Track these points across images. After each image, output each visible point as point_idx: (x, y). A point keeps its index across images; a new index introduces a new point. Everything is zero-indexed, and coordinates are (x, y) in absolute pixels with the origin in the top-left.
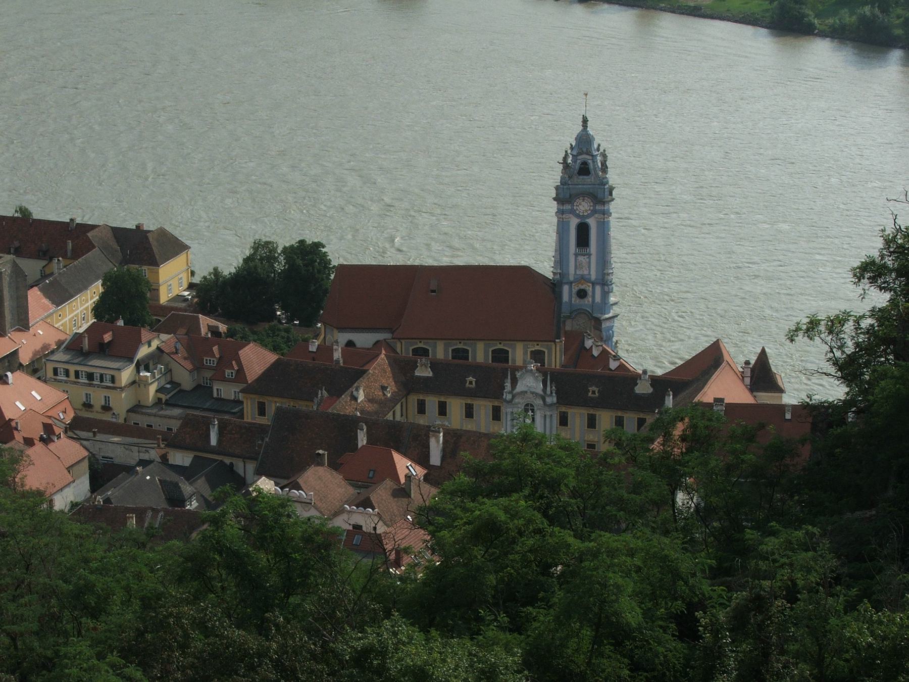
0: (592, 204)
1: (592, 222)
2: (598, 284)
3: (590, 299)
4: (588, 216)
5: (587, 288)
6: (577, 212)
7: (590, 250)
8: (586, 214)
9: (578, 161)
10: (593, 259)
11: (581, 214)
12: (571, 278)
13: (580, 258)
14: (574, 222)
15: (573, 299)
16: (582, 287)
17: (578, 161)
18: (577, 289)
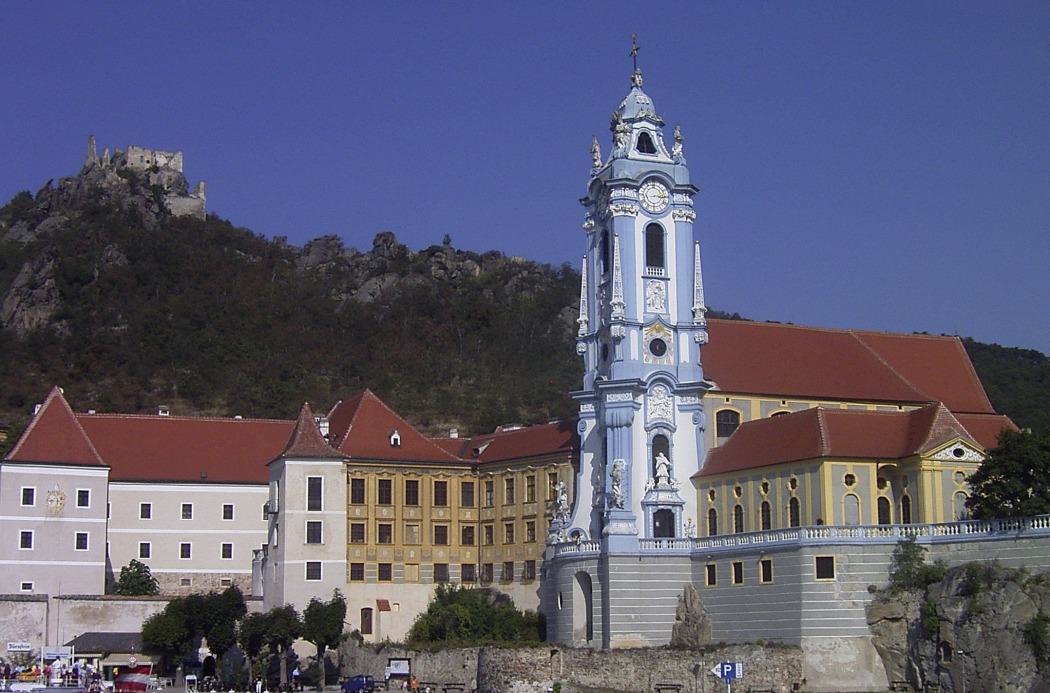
0: (667, 193)
1: (668, 224)
2: (684, 328)
3: (672, 359)
4: (662, 214)
5: (665, 339)
6: (645, 205)
7: (666, 273)
8: (657, 210)
9: (635, 132)
10: (672, 284)
11: (651, 209)
13: (653, 286)
14: (641, 222)
15: (645, 356)
17: (635, 132)
18: (651, 339)
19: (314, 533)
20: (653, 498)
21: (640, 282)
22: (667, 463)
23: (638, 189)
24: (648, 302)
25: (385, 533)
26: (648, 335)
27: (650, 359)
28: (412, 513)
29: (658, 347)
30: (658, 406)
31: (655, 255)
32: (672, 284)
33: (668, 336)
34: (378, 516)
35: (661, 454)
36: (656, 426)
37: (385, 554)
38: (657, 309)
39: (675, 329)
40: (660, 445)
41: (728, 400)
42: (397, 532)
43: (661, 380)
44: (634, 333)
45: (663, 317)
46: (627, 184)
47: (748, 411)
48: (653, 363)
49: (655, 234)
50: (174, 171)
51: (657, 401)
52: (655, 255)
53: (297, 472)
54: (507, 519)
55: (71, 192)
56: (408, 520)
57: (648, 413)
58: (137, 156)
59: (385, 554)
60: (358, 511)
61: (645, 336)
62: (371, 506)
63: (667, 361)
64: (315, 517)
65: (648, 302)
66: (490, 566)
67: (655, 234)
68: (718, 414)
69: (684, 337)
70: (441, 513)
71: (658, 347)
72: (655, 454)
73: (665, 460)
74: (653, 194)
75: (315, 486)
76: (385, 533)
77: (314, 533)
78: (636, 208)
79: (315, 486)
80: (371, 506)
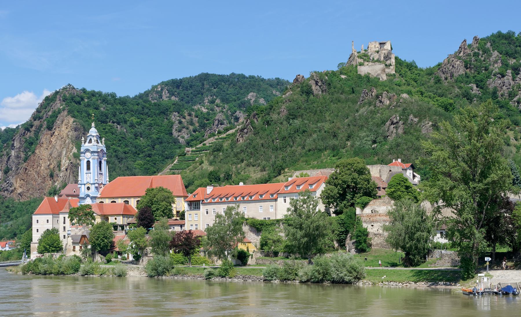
1: (91, 160)
11: (88, 157)
12: (85, 183)
14: (86, 160)
16: (88, 186)
21: (85, 175)
23: (85, 153)
26: (87, 186)
27: (86, 190)
29: (88, 188)
31: (88, 168)
32: (92, 174)
33: (90, 186)
38: (88, 180)
39: (92, 184)
43: (88, 196)
44: (83, 186)
46: (82, 153)
47: (105, 201)
48: (87, 192)
49: (88, 163)
50: (387, 50)
52: (88, 168)
53: (61, 216)
55: (300, 80)
58: (373, 46)
63: (90, 191)
64: (64, 225)
67: (88, 163)
69: (93, 185)
71: (88, 188)
74: (88, 155)
75: (64, 218)
78: (84, 158)
79: (64, 218)
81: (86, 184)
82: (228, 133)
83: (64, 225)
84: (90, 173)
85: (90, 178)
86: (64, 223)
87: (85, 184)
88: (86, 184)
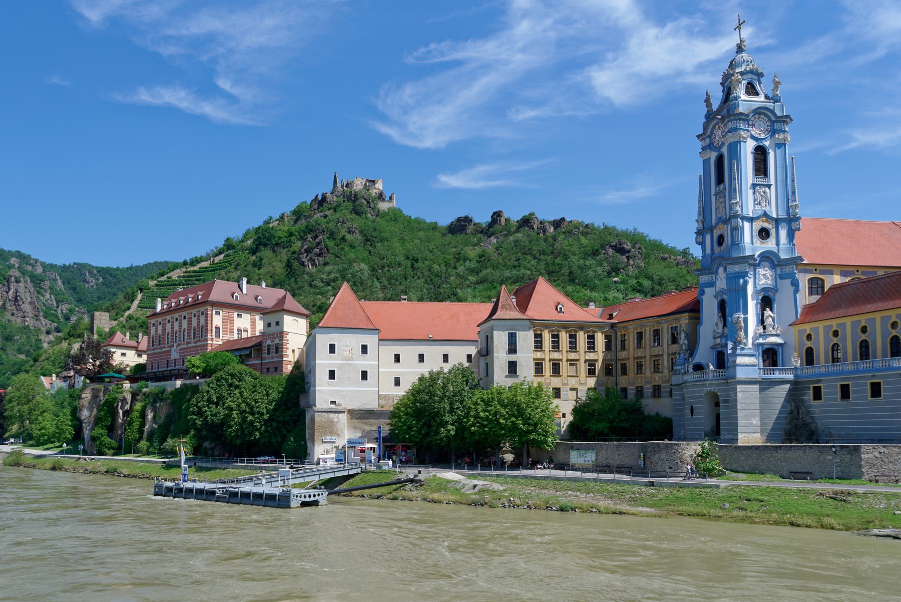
3: (774, 241)
15: (754, 240)
18: (759, 227)
19: (513, 367)
20: (761, 341)
22: (772, 315)
24: (756, 202)
25: (556, 368)
26: (757, 225)
27: (758, 242)
28: (573, 356)
29: (764, 234)
30: (764, 277)
34: (552, 357)
35: (768, 309)
36: (763, 289)
37: (556, 382)
39: (777, 222)
40: (766, 302)
41: (816, 270)
42: (564, 367)
43: (768, 258)
44: (747, 225)
45: (768, 212)
51: (765, 272)
54: (638, 358)
56: (571, 360)
57: (757, 281)
59: (556, 382)
60: (539, 355)
61: (754, 226)
62: (547, 350)
63: (770, 245)
64: (512, 357)
65: (756, 202)
66: (624, 390)
68: (809, 280)
70: (592, 354)
71: (764, 234)
72: (763, 310)
73: (770, 313)
76: (556, 368)
77: (513, 367)
80: (547, 350)
81: (758, 218)
82: (199, 266)
83: (512, 357)
84: (769, 186)
85: (769, 203)
86: (512, 350)
87: (751, 220)
88: (758, 218)
